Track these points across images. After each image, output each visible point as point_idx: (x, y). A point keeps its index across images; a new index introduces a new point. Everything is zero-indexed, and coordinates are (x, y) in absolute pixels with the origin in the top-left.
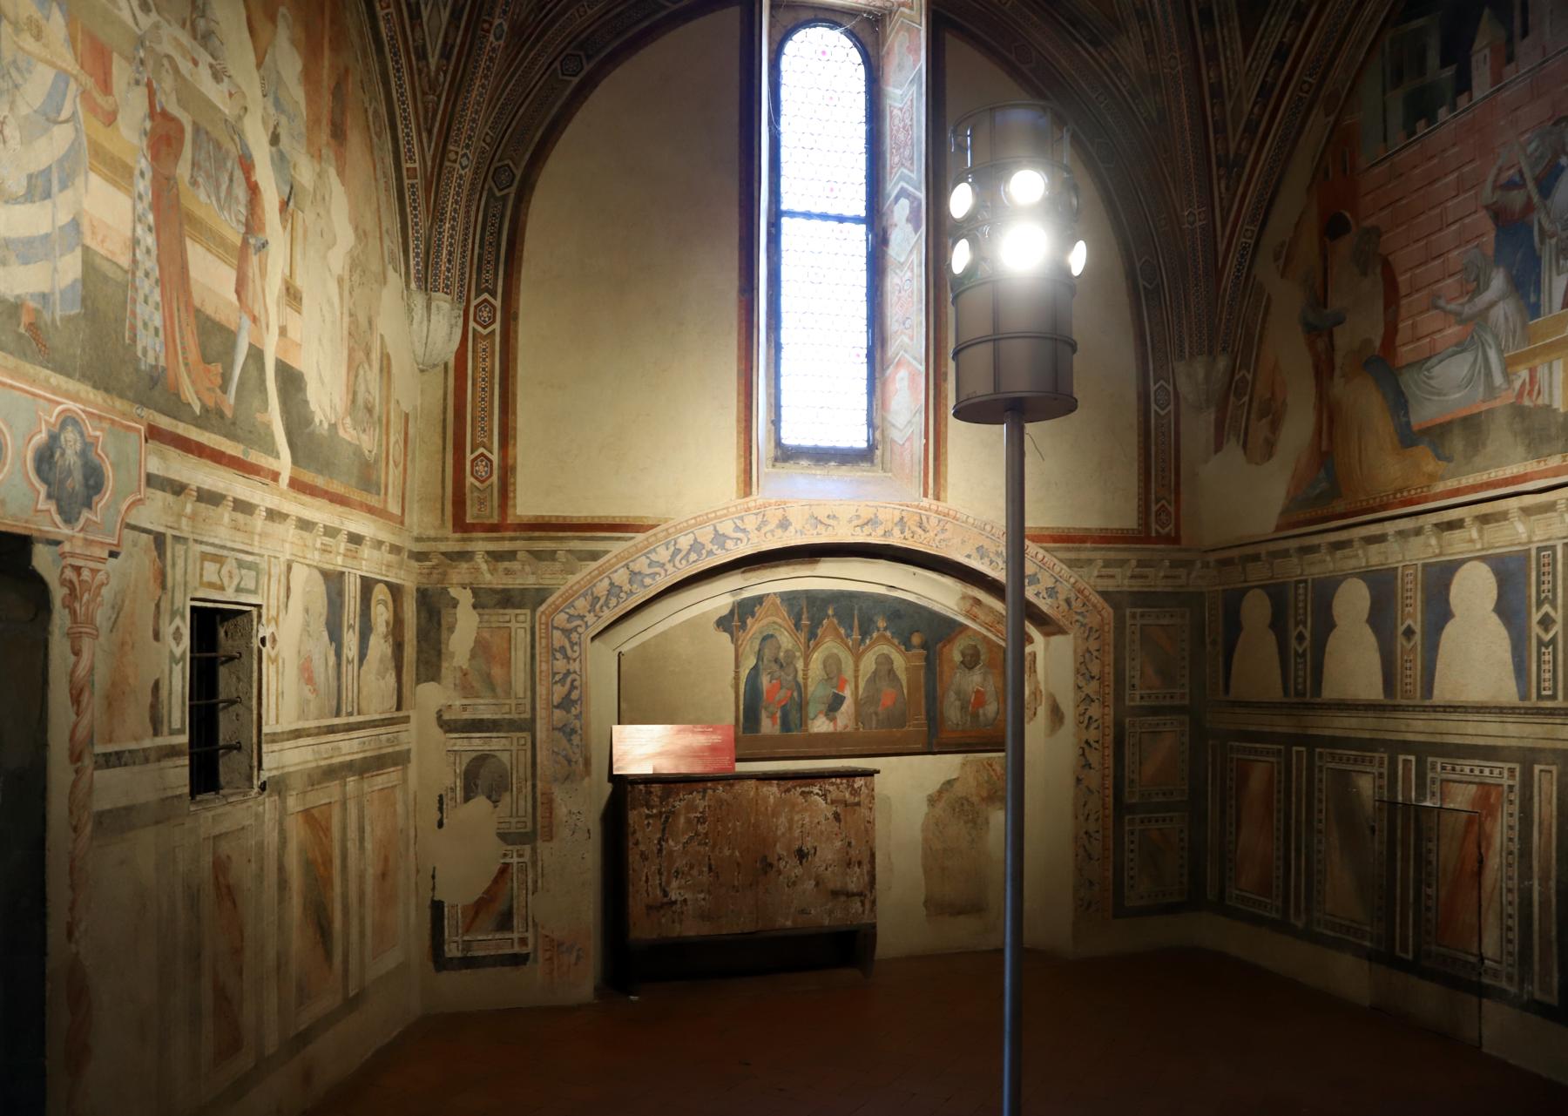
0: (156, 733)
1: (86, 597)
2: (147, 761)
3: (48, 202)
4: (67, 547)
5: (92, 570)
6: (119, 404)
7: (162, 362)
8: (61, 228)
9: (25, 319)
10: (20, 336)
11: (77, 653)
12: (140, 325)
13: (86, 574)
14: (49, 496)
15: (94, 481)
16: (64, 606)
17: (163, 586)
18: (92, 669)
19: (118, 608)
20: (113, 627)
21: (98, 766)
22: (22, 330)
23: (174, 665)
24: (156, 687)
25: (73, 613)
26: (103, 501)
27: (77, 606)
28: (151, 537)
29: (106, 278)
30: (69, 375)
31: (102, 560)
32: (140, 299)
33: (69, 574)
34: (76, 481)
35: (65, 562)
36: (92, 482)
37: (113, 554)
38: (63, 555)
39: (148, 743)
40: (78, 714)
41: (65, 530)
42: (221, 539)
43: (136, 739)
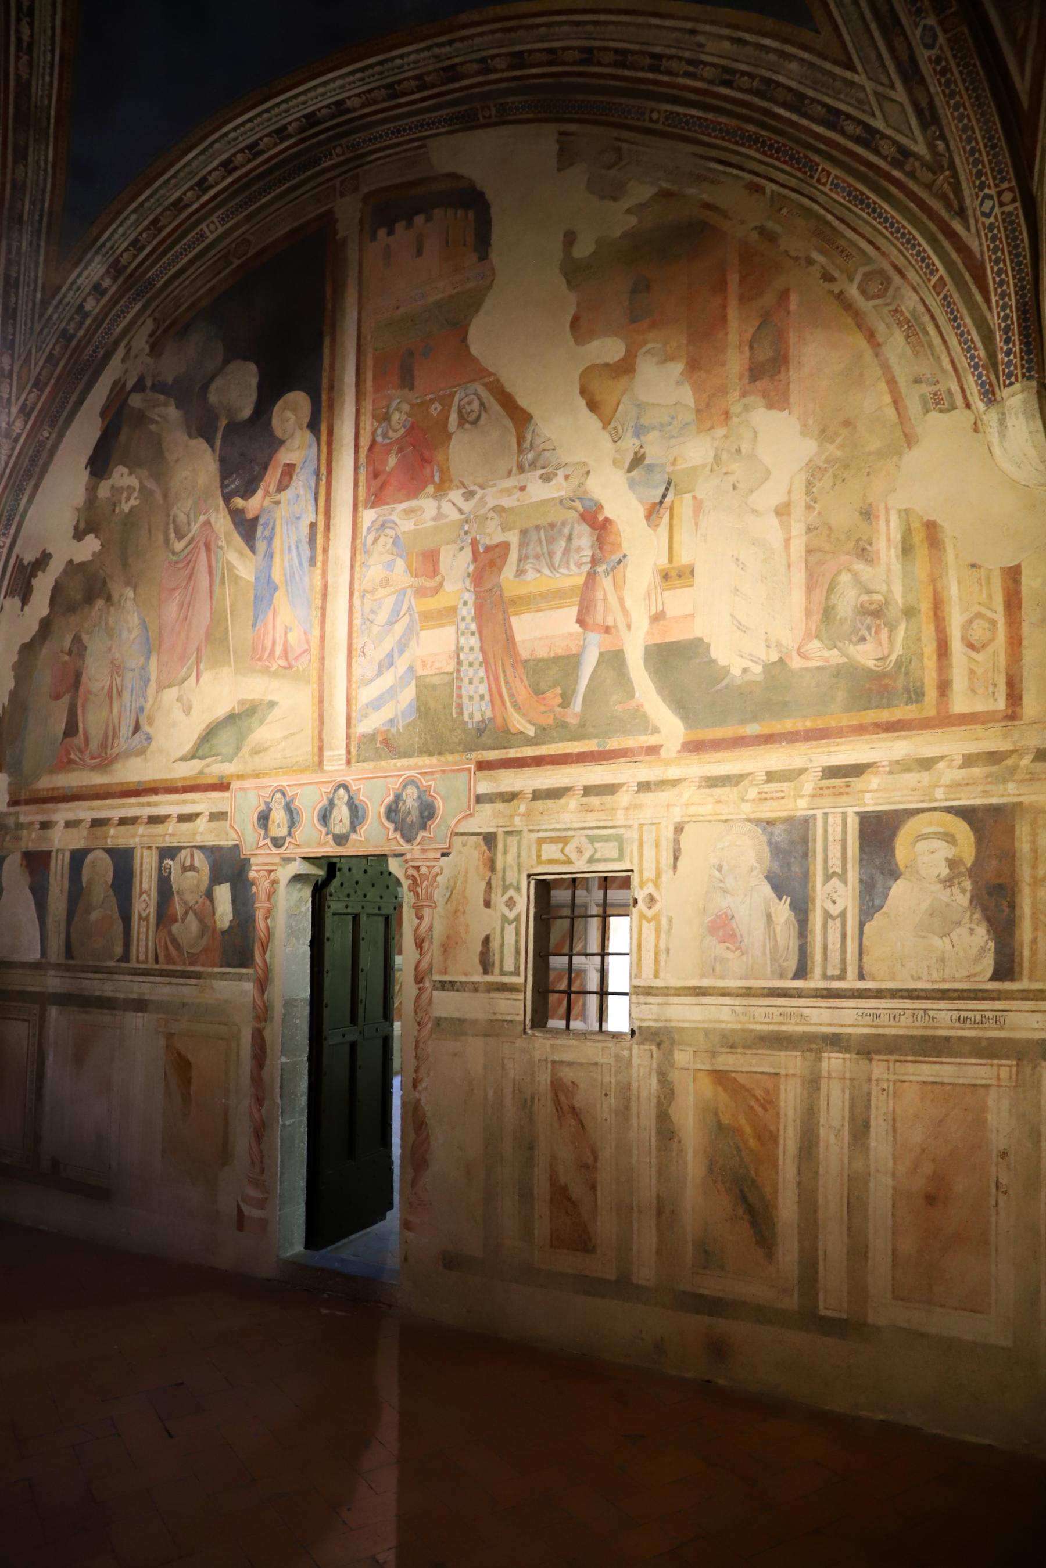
0: (486, 972)
1: (425, 884)
2: (476, 990)
3: (392, 669)
4: (408, 856)
5: (428, 867)
6: (450, 758)
7: (489, 714)
8: (401, 677)
9: (380, 738)
10: (377, 749)
11: (420, 918)
12: (465, 700)
13: (424, 870)
14: (396, 830)
15: (427, 812)
16: (410, 891)
17: (493, 869)
18: (431, 928)
19: (451, 889)
20: (448, 900)
21: (435, 988)
22: (378, 745)
23: (506, 925)
24: (487, 940)
25: (417, 894)
26: (433, 825)
27: (419, 890)
28: (481, 837)
29: (434, 687)
30: (410, 757)
31: (437, 860)
32: (466, 680)
33: (411, 871)
34: (414, 816)
35: (407, 865)
36: (426, 814)
37: (443, 855)
38: (406, 862)
39: (478, 978)
40: (421, 954)
41: (407, 847)
42: (565, 823)
43: (466, 974)
